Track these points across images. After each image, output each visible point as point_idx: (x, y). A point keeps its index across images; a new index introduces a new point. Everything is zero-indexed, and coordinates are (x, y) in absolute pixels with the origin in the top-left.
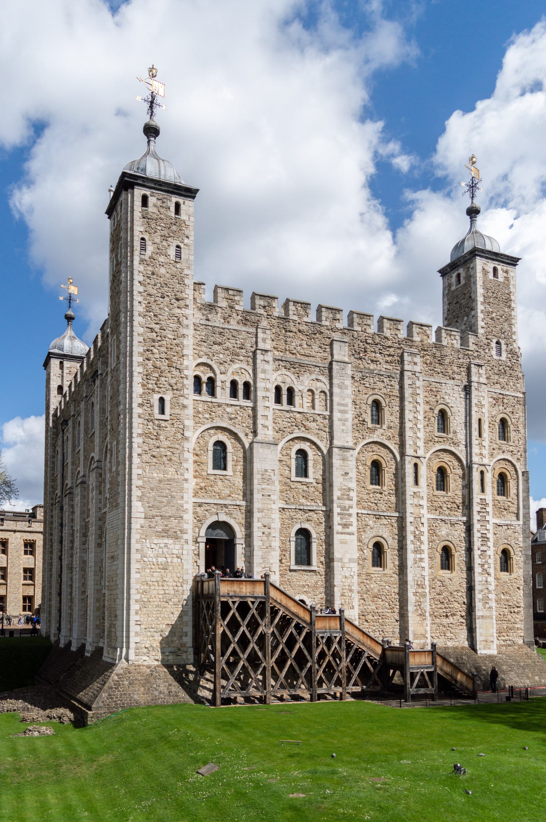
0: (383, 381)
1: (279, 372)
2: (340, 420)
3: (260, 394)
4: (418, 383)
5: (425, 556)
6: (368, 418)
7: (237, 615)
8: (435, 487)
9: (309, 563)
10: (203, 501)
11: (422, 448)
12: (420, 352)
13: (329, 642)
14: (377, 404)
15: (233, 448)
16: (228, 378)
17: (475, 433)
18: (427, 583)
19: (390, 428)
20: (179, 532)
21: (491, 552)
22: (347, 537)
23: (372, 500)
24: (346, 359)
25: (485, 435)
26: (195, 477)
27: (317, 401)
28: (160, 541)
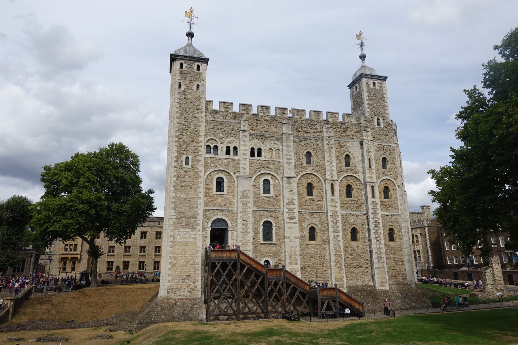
1: (253, 141)
2: (287, 163)
3: (242, 152)
4: (331, 142)
5: (340, 234)
6: (304, 161)
7: (220, 269)
8: (345, 195)
9: (271, 240)
10: (210, 208)
11: (336, 176)
13: (276, 284)
14: (309, 154)
15: (228, 180)
16: (224, 146)
17: (367, 166)
18: (342, 249)
20: (195, 225)
21: (381, 231)
22: (293, 224)
23: (308, 204)
24: (290, 132)
25: (373, 167)
26: (206, 196)
27: (274, 154)
28: (184, 230)
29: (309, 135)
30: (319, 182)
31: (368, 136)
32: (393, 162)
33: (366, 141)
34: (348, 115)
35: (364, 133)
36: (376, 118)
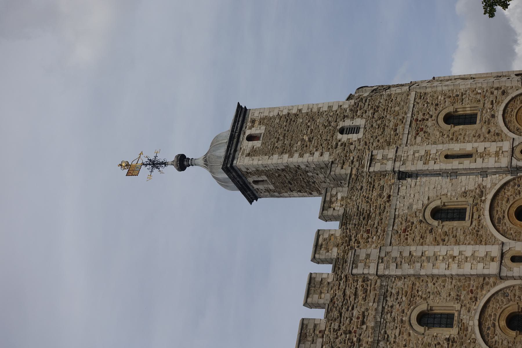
0: (392, 307)
6: (444, 333)
11: (489, 248)
12: (352, 248)
14: (427, 319)
17: (467, 163)
19: (458, 298)
25: (468, 147)
29: (372, 313)
30: (505, 295)
31: (384, 157)
32: (459, 97)
33: (398, 164)
34: (326, 206)
35: (377, 167)
36: (339, 136)
